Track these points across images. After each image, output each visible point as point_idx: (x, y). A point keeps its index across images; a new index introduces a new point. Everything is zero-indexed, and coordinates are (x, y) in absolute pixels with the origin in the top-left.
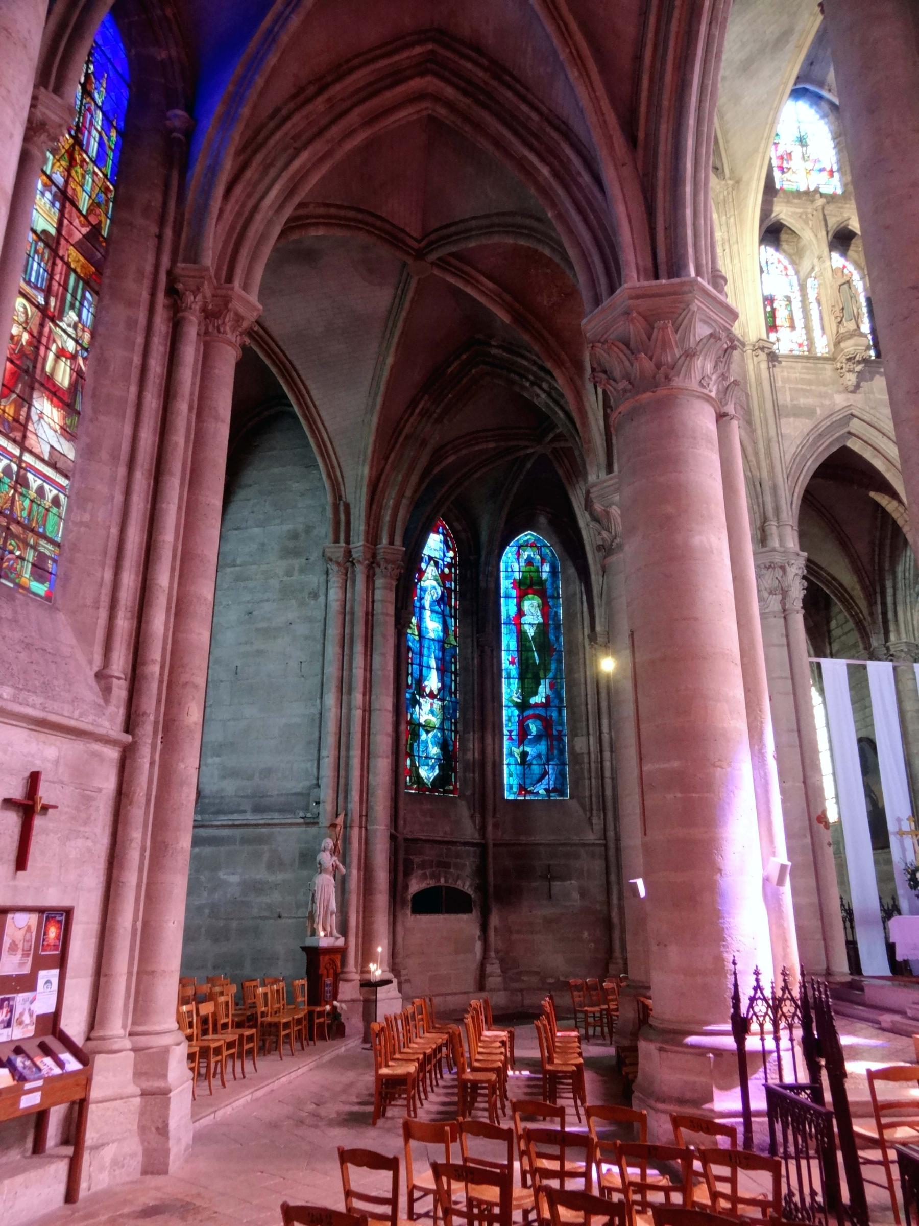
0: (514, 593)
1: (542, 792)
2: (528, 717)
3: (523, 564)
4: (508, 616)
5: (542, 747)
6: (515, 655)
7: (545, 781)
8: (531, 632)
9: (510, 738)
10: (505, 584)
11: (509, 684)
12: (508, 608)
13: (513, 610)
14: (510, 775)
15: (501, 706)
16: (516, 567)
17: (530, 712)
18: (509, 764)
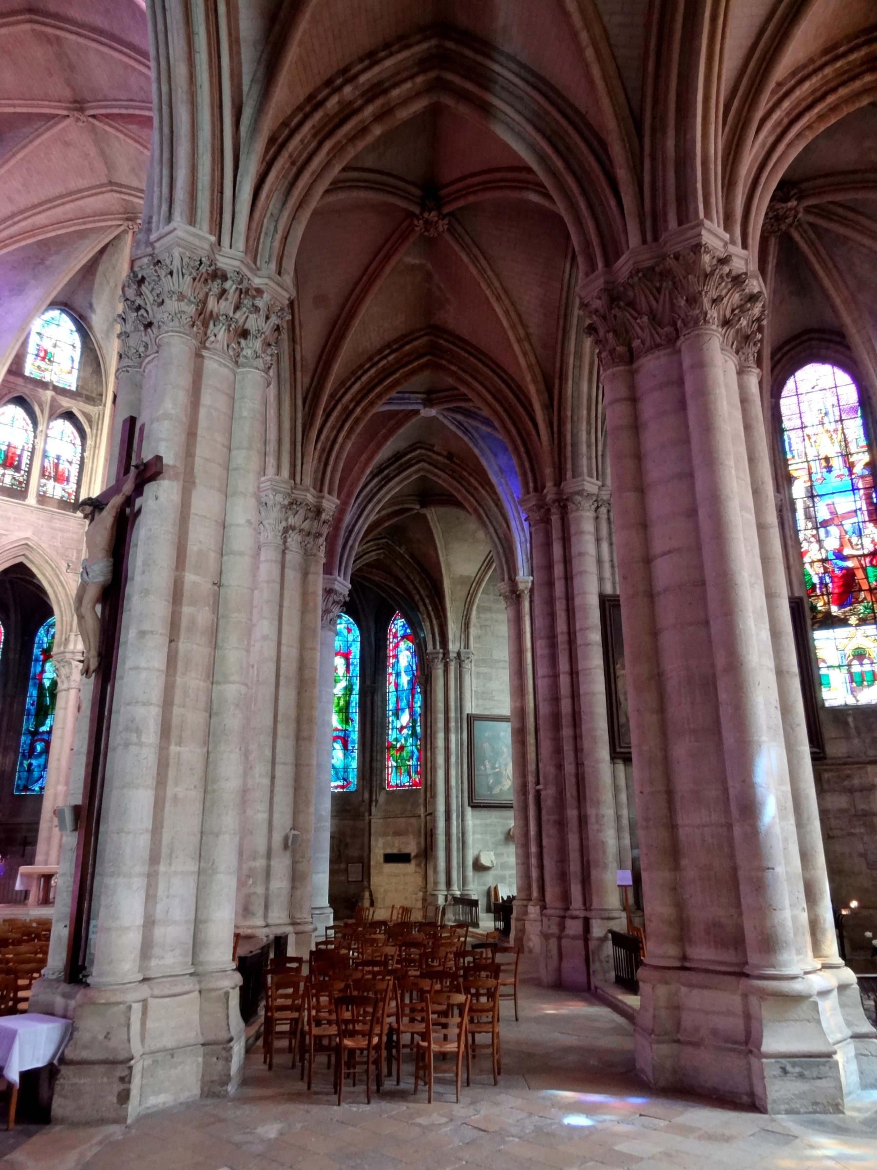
0: (41, 657)
1: (37, 789)
2: (37, 740)
3: (50, 638)
4: (35, 674)
5: (42, 760)
6: (36, 699)
7: (40, 782)
8: (47, 683)
9: (24, 755)
10: (37, 651)
11: (28, 720)
12: (36, 669)
13: (39, 669)
14: (20, 778)
15: (20, 734)
16: (45, 639)
17: (39, 737)
18: (19, 772)
